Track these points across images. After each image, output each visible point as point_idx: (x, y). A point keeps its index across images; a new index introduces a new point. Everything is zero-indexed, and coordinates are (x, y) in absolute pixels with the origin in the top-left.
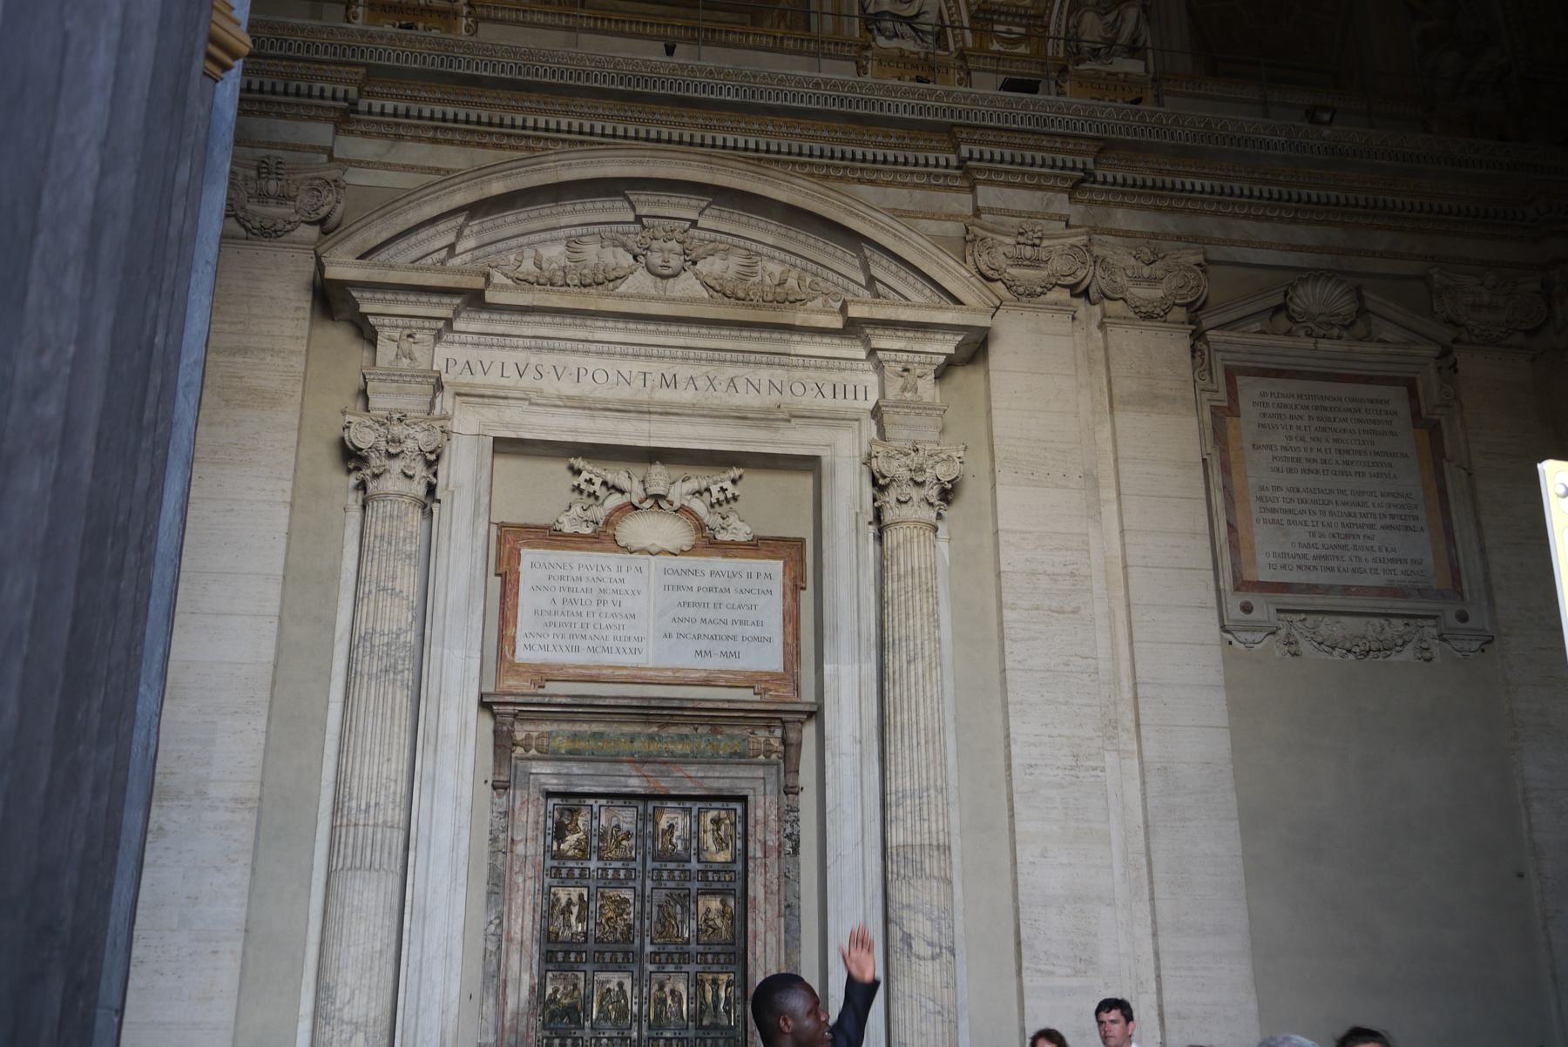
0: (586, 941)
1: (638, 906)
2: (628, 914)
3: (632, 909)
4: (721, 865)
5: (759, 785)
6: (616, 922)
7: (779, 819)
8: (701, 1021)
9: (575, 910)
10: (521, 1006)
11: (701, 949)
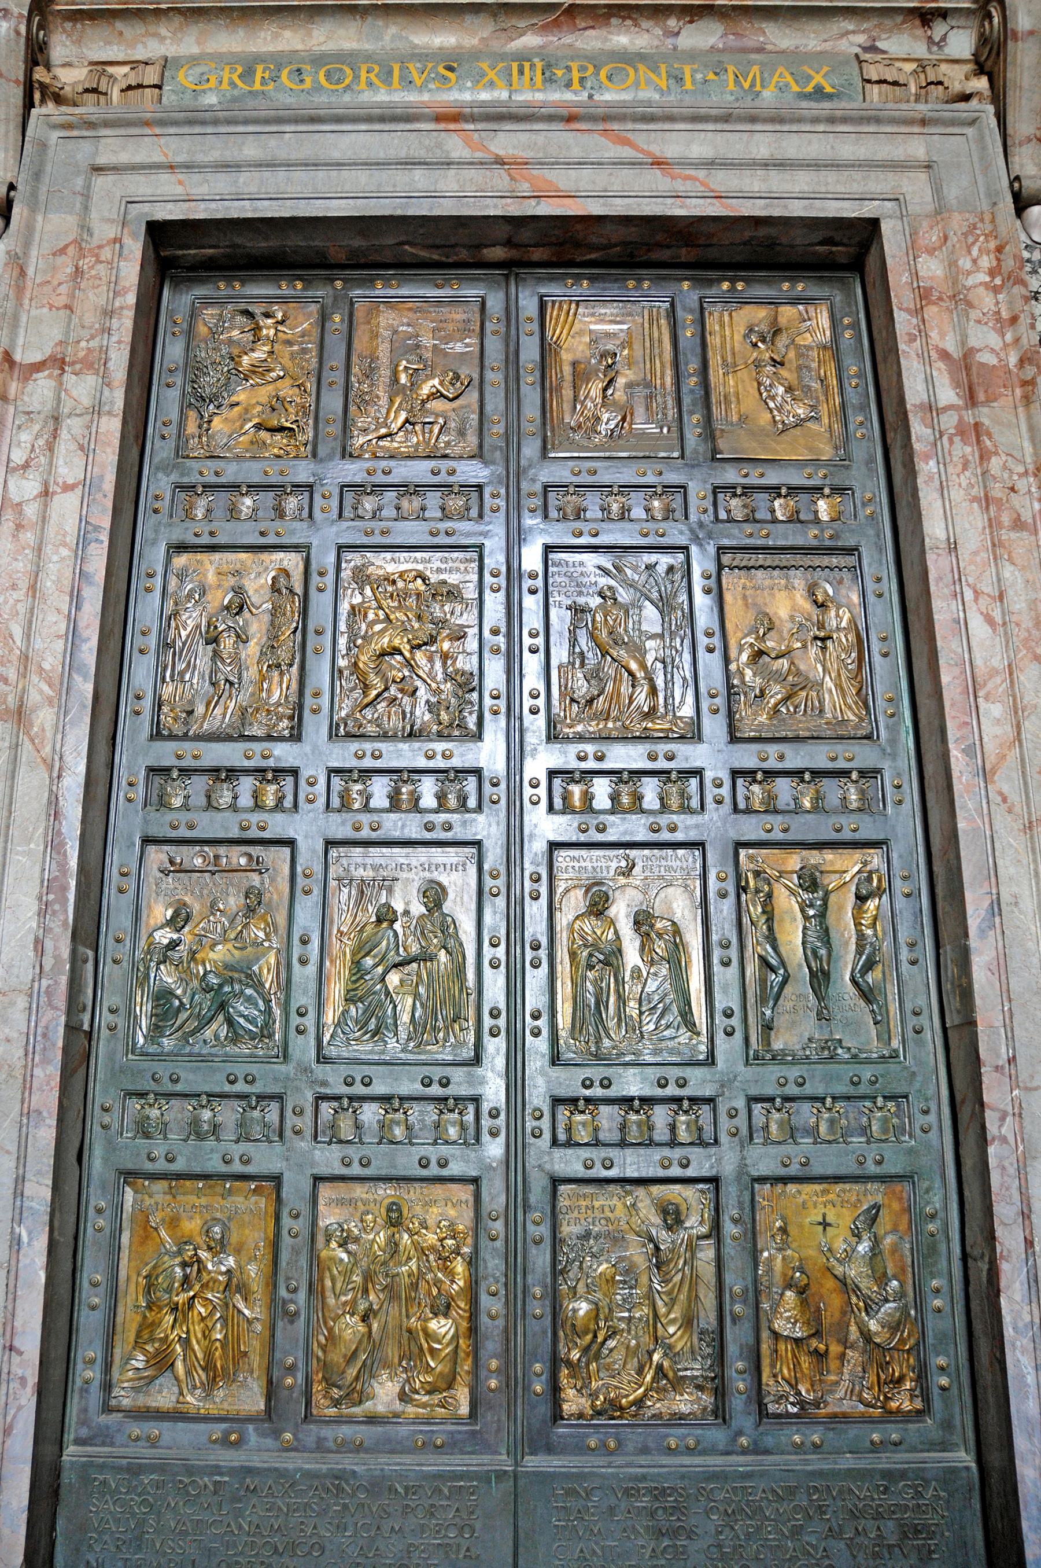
0: (296, 736)
1: (495, 606)
2: (459, 636)
3: (469, 618)
9: (257, 627)
11: (747, 757)
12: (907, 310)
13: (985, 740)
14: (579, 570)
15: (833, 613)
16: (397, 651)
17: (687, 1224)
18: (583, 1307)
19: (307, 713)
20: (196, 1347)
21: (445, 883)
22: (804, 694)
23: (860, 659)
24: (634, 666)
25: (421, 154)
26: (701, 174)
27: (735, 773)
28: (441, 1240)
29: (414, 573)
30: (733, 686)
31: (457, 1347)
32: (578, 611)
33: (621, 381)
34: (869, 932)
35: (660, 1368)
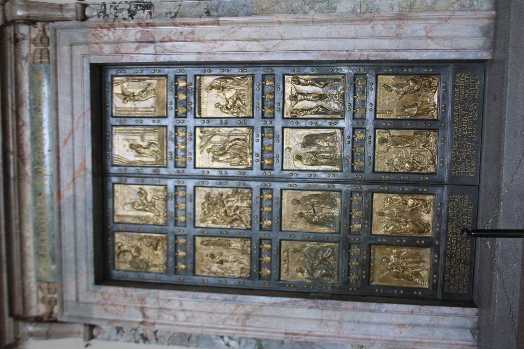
1: (211, 183)
3: (216, 192)
4: (170, 93)
5: (79, 51)
6: (230, 207)
7: (112, 26)
8: (335, 113)
10: (313, 317)
11: (258, 113)
12: (122, 58)
13: (258, 50)
14: (201, 158)
15: (215, 85)
16: (225, 212)
17: (386, 138)
18: (407, 165)
19: (244, 236)
20: (414, 266)
21: (292, 198)
22: (239, 96)
23: (230, 78)
24: (230, 144)
25: (71, 204)
26: (76, 118)
27: (263, 117)
28: (388, 202)
29: (202, 206)
30: (237, 116)
31: (417, 199)
32: (214, 159)
33: (141, 143)
34: (308, 81)
35: (423, 146)
